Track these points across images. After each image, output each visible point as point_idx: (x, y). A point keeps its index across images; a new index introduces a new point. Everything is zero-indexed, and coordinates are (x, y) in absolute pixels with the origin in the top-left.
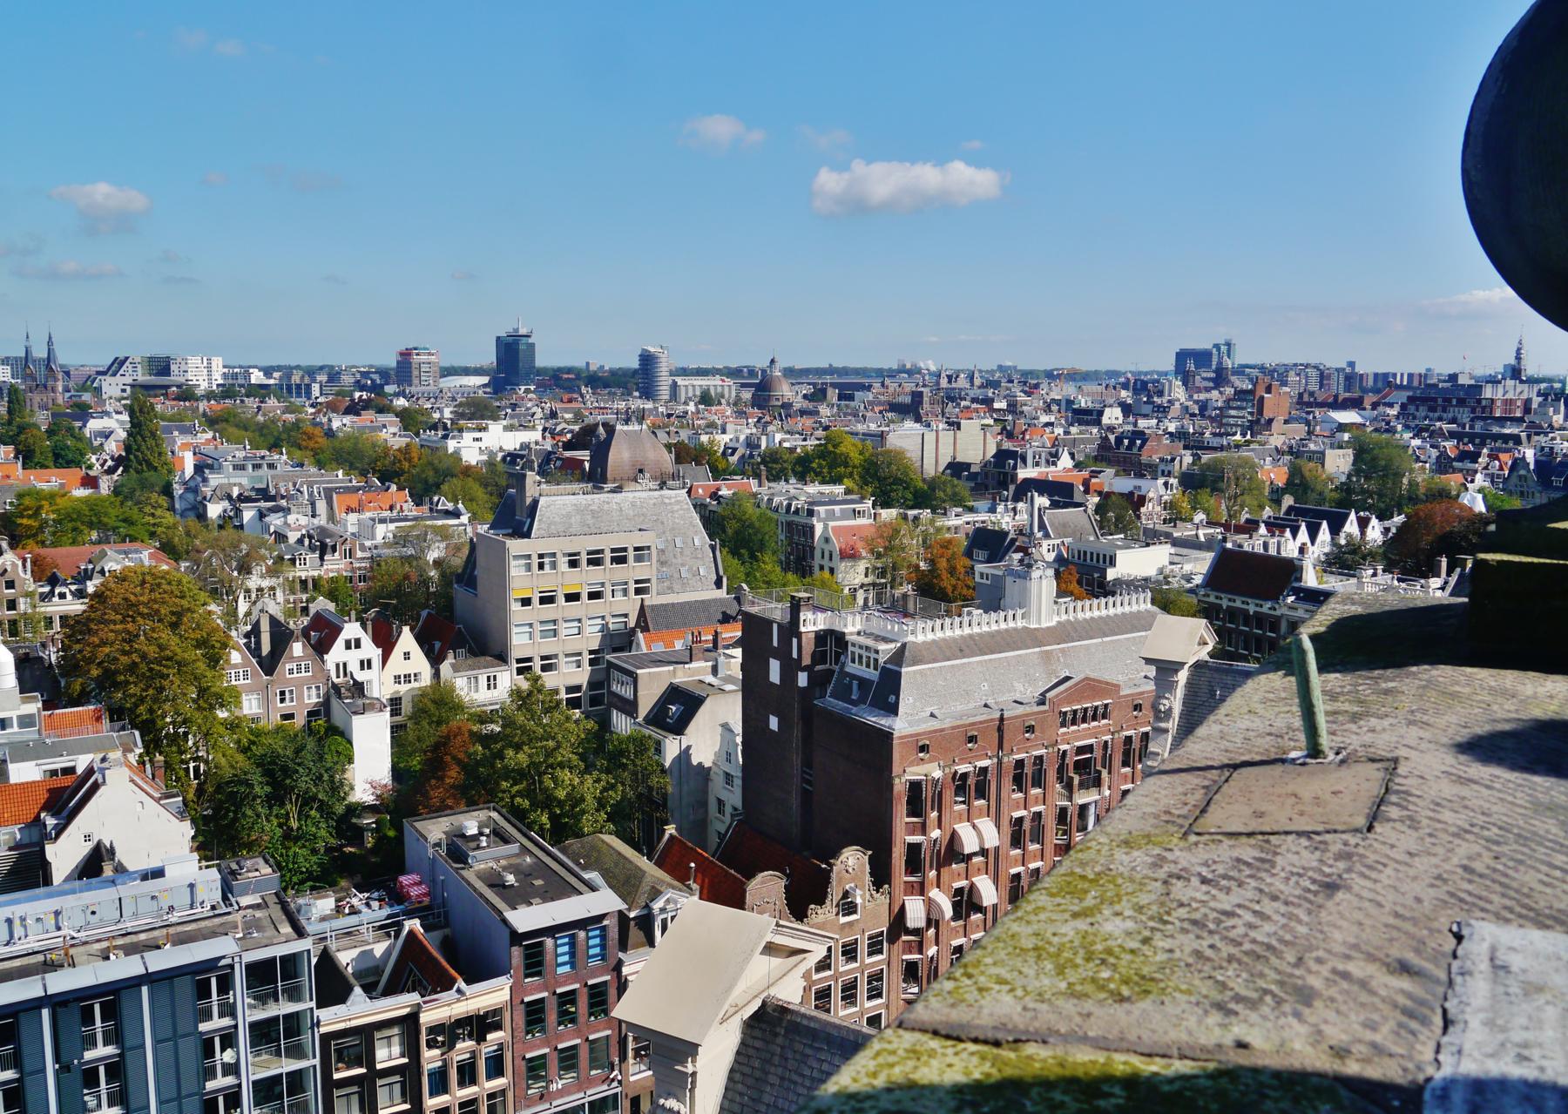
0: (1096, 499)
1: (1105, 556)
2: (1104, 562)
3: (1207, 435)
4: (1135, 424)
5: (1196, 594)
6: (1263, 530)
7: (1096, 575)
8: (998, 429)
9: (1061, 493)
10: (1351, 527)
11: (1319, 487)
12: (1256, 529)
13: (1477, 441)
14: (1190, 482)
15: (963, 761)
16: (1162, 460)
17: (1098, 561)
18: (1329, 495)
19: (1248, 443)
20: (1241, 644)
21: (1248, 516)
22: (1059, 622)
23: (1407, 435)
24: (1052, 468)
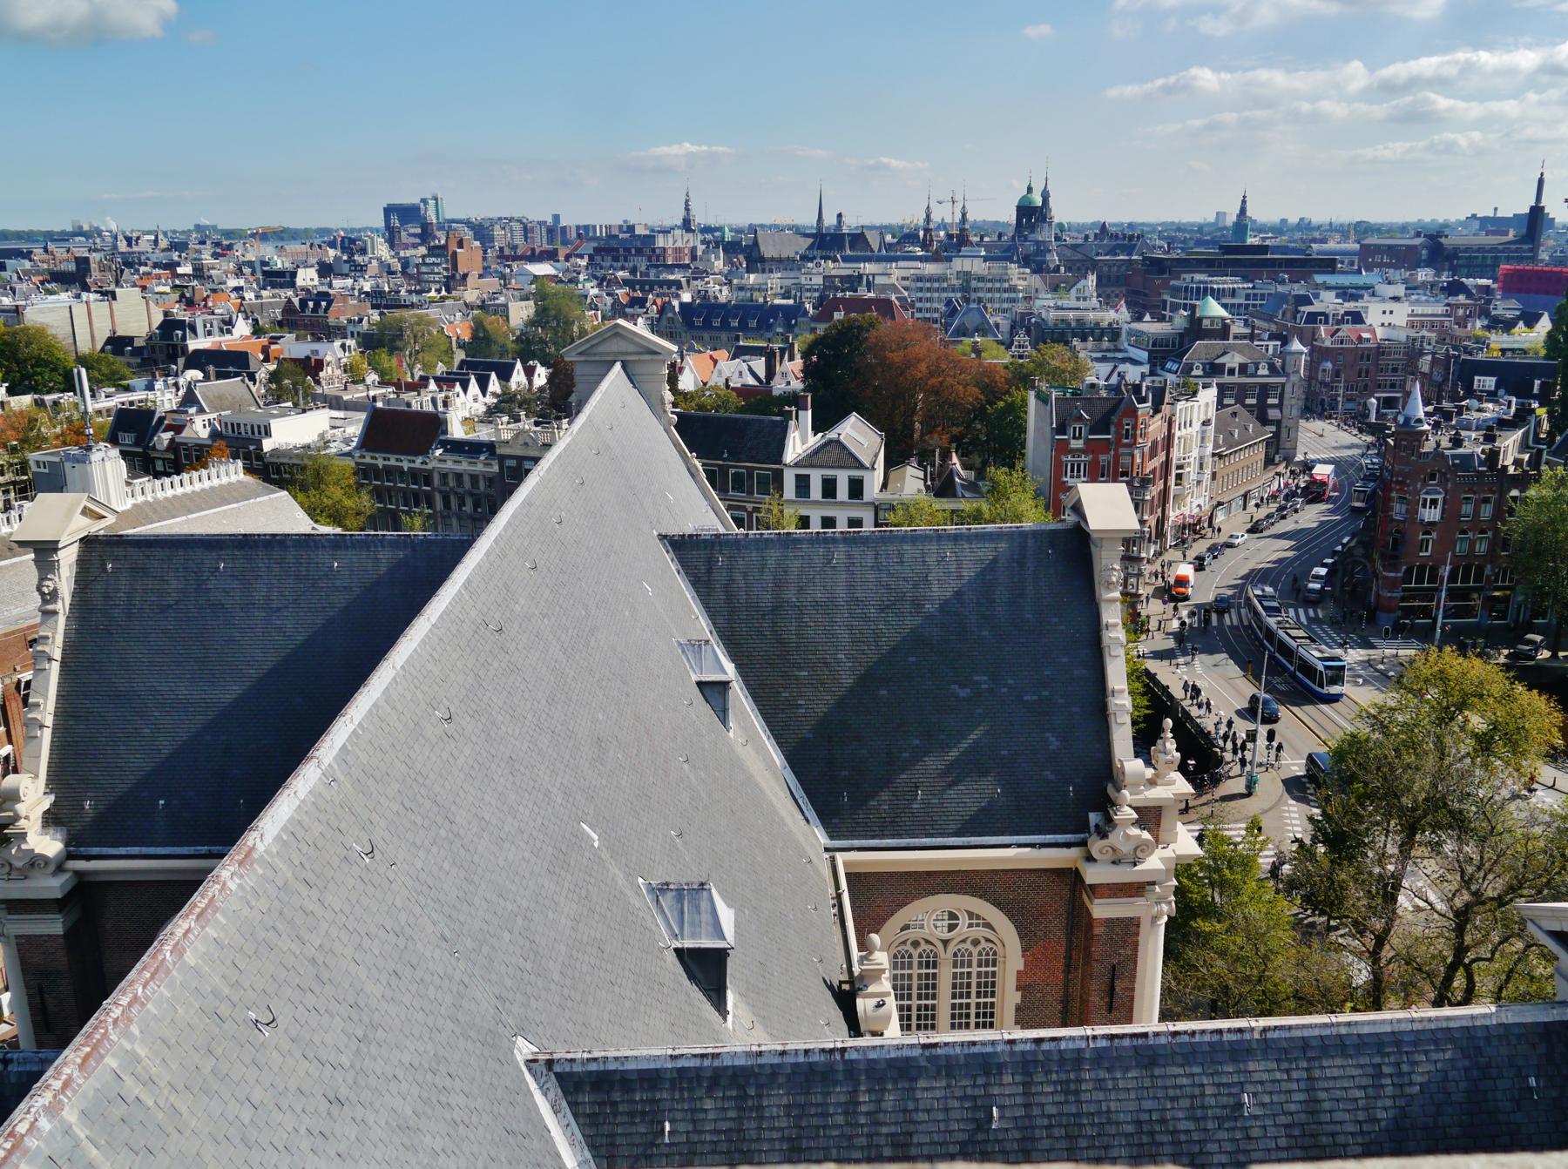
0: (272, 367)
1: (259, 427)
2: (260, 433)
3: (403, 292)
4: (330, 286)
5: (353, 457)
6: (432, 386)
7: (252, 448)
8: (176, 296)
9: (228, 363)
10: (518, 378)
11: (501, 340)
12: (426, 386)
13: (647, 287)
14: (370, 342)
15: (25, 668)
16: (350, 321)
17: (253, 433)
18: (511, 346)
19: (443, 299)
20: (401, 501)
21: (421, 373)
22: (135, 505)
23: (588, 285)
24: (228, 337)
